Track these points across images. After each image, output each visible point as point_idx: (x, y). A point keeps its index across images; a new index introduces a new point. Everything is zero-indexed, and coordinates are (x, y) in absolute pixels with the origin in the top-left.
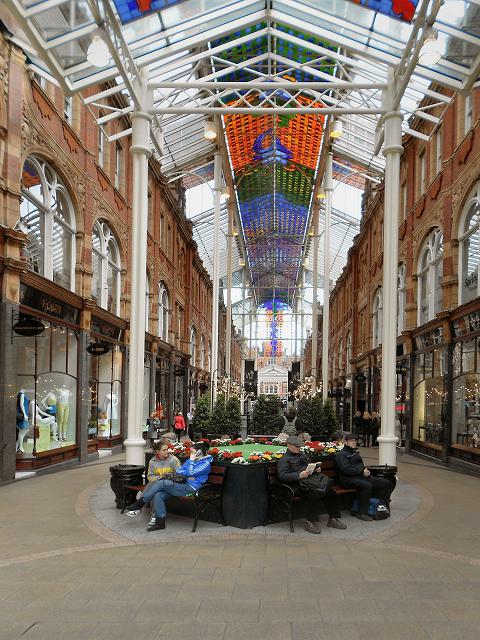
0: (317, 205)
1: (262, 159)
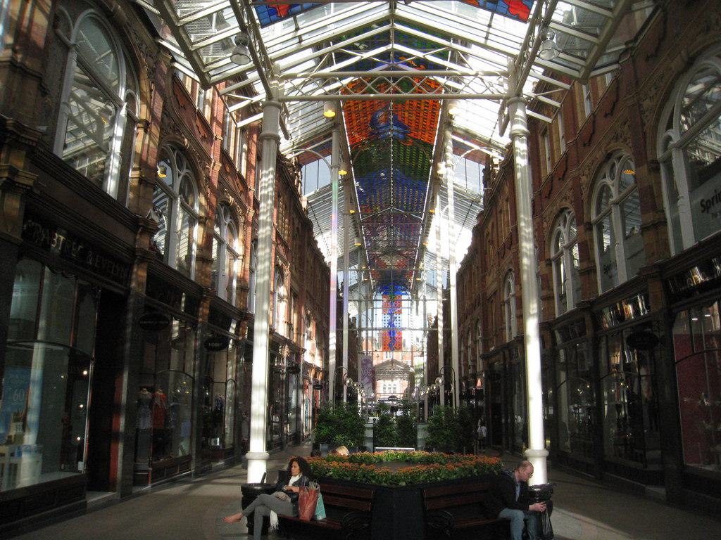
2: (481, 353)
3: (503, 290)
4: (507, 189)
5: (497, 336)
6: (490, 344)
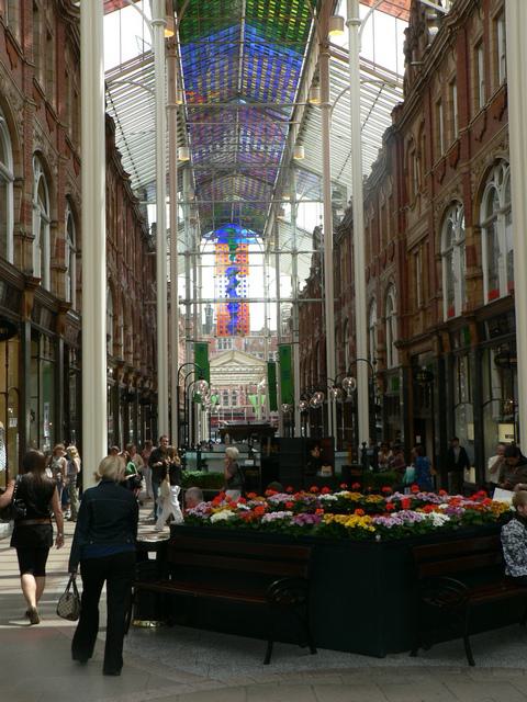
2: (395, 338)
4: (452, 65)
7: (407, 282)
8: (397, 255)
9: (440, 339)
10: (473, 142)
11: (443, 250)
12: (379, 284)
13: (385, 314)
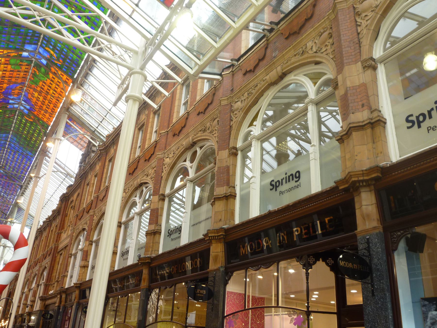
0: (45, 152)
1: (8, 103)
2: (41, 295)
3: (74, 245)
4: (98, 167)
5: (58, 281)
6: (51, 288)
7: (53, 267)
8: (52, 253)
9: (61, 297)
10: (99, 201)
11: (74, 252)
12: (40, 267)
13: (39, 282)
